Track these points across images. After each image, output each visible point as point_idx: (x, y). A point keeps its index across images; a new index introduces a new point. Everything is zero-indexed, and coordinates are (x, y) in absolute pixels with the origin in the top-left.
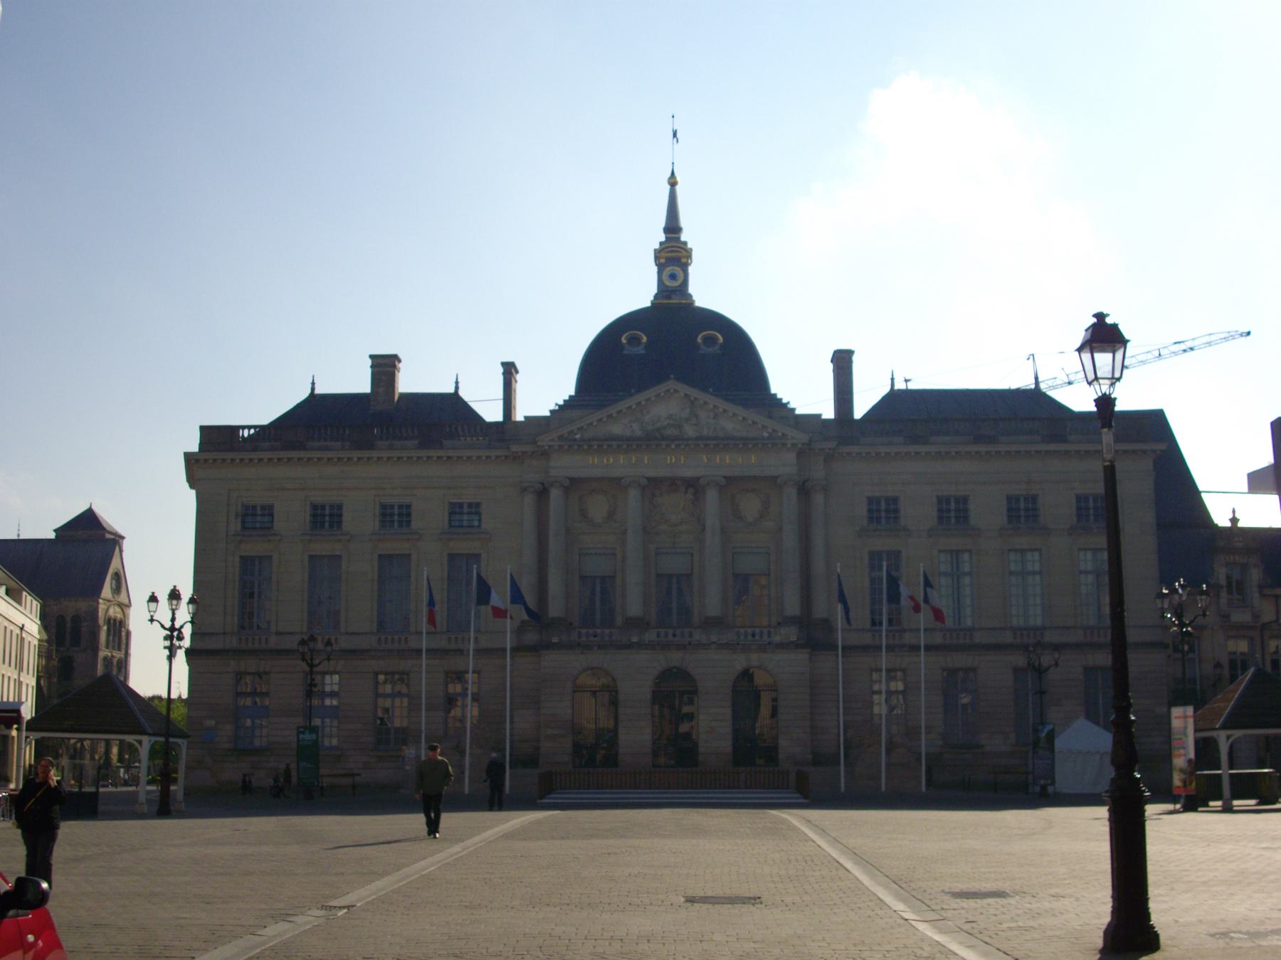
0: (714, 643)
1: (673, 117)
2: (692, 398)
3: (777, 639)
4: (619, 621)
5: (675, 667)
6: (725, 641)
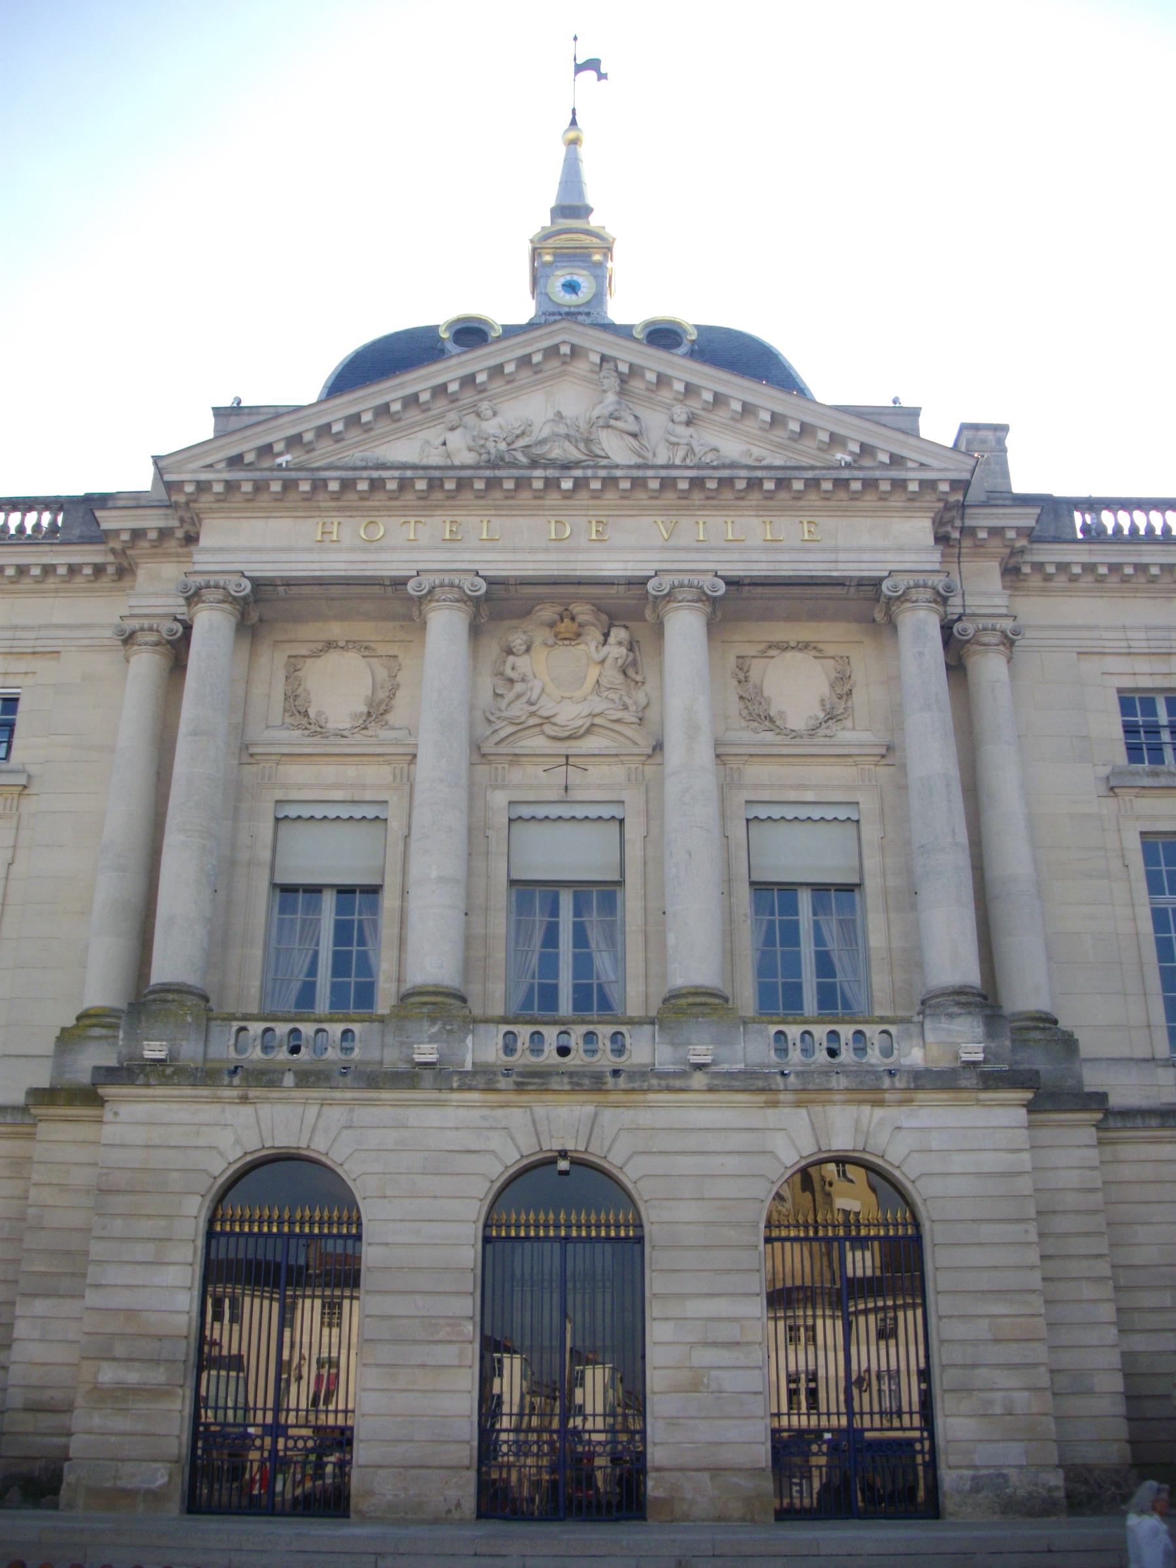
0: (700, 1067)
1: (575, 39)
2: (624, 368)
3: (914, 1056)
4: (384, 1003)
5: (563, 1154)
6: (742, 1066)
